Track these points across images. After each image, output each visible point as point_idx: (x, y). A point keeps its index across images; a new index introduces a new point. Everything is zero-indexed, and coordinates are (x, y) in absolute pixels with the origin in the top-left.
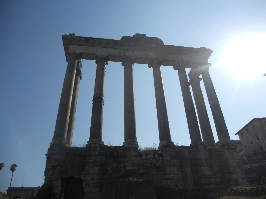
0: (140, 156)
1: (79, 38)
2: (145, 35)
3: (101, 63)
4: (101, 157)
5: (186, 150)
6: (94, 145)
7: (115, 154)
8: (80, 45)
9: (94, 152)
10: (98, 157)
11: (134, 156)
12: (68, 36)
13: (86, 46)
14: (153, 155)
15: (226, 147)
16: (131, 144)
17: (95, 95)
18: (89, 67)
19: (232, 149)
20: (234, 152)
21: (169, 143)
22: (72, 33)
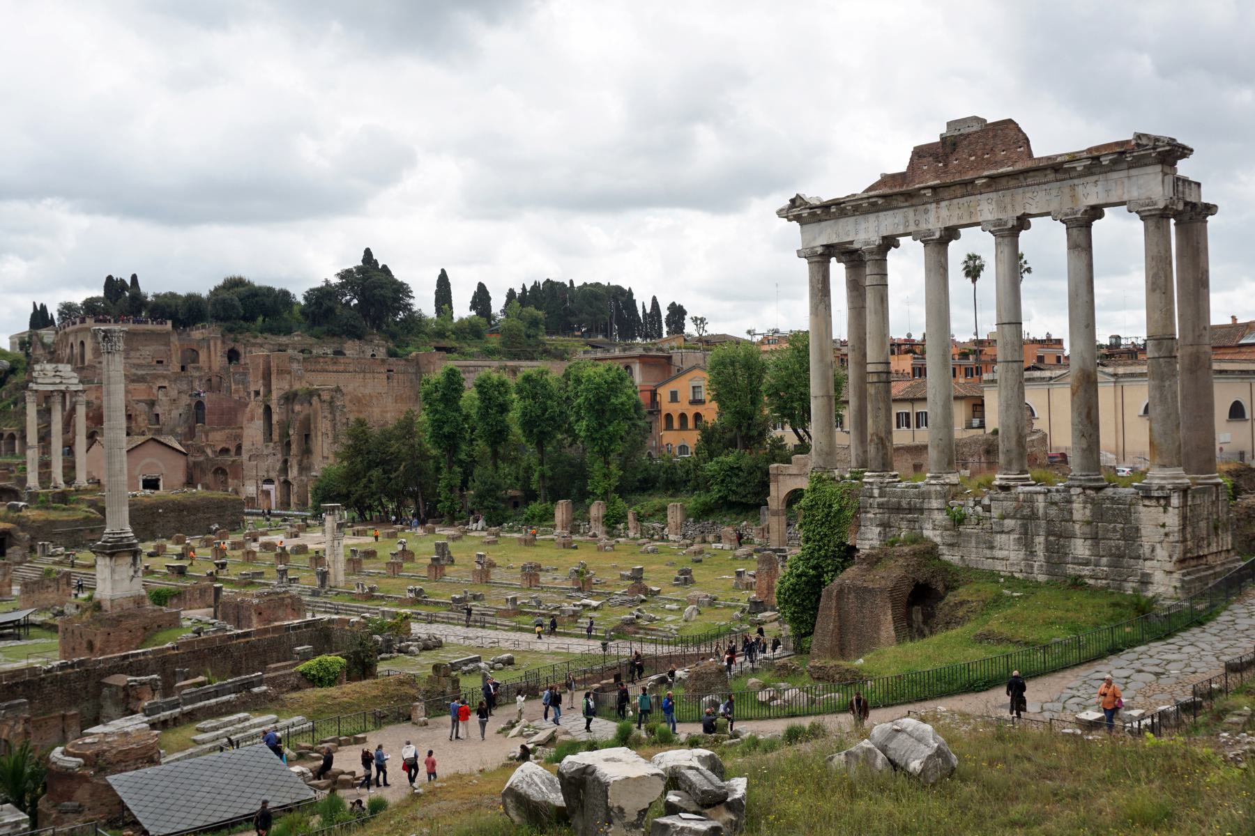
5: (1041, 498)
19: (1158, 498)
21: (1004, 483)
22: (794, 196)
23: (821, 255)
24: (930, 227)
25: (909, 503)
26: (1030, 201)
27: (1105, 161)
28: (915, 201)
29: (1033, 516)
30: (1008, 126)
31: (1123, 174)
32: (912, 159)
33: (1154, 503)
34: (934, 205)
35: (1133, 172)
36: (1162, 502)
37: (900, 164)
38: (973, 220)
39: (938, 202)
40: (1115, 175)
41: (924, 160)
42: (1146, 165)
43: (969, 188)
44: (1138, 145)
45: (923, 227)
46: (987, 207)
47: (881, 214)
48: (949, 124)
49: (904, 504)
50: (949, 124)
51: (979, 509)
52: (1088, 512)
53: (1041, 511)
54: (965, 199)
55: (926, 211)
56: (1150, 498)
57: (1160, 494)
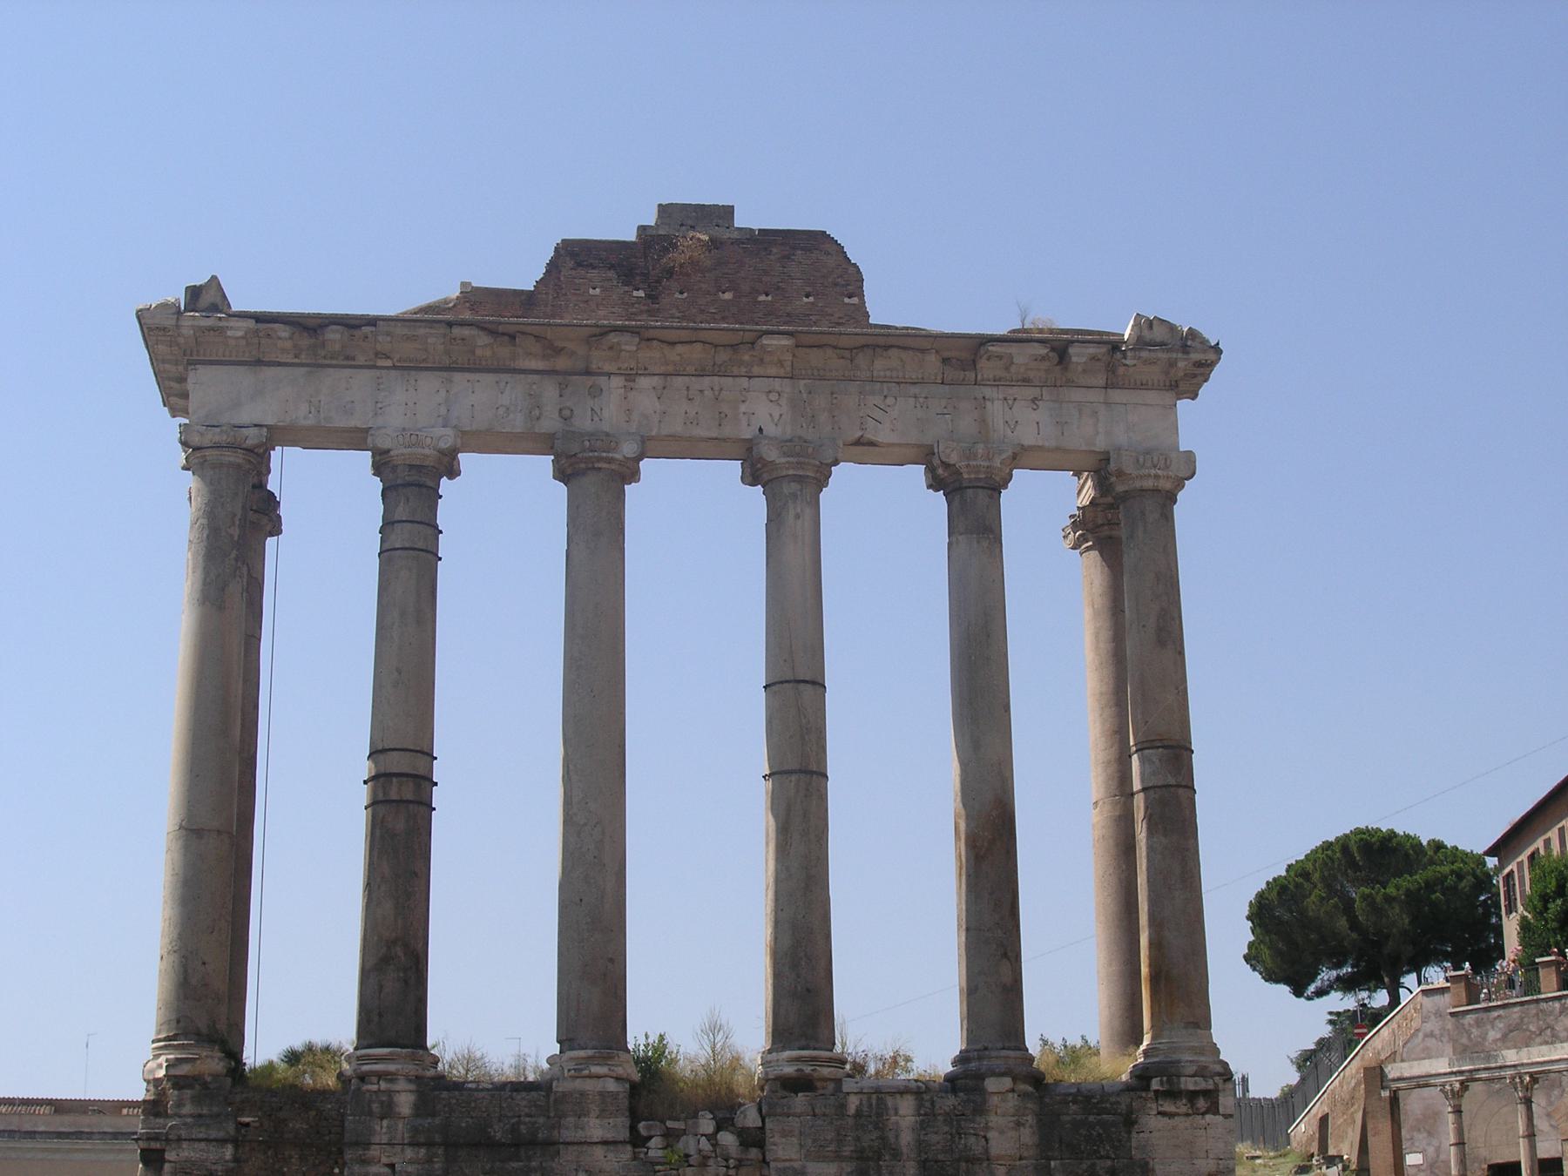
0: (635, 1146)
1: (251, 323)
2: (728, 211)
3: (412, 489)
4: (423, 1151)
5: (906, 1106)
6: (383, 1085)
7: (499, 1135)
8: (259, 363)
9: (385, 1123)
10: (409, 1153)
11: (605, 1143)
12: (178, 300)
13: (302, 365)
14: (711, 1138)
15: (1155, 1084)
16: (590, 1077)
17: (384, 751)
18: (327, 503)
19: (1193, 1096)
20: (1203, 1114)
21: (808, 1069)
22: (201, 279)
23: (249, 450)
24: (606, 427)
25: (514, 1129)
26: (878, 414)
27: (1078, 355)
28: (562, 363)
29: (887, 1148)
30: (818, 242)
31: (1095, 396)
32: (553, 267)
33: (1182, 1106)
34: (617, 382)
35: (1117, 395)
36: (1201, 1103)
37: (522, 271)
38: (727, 431)
39: (630, 377)
40: (1076, 395)
41: (593, 274)
42: (1143, 386)
43: (723, 356)
44: (1140, 343)
45: (583, 423)
46: (765, 412)
47: (457, 376)
48: (664, 210)
49: (498, 1132)
50: (664, 210)
51: (727, 1139)
52: (1028, 1136)
53: (906, 1139)
54: (707, 380)
55: (595, 392)
56: (1172, 1094)
57: (1202, 1084)
